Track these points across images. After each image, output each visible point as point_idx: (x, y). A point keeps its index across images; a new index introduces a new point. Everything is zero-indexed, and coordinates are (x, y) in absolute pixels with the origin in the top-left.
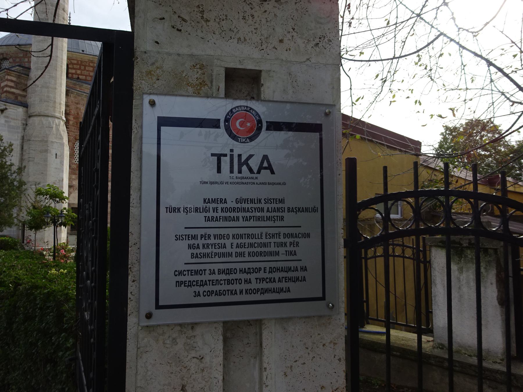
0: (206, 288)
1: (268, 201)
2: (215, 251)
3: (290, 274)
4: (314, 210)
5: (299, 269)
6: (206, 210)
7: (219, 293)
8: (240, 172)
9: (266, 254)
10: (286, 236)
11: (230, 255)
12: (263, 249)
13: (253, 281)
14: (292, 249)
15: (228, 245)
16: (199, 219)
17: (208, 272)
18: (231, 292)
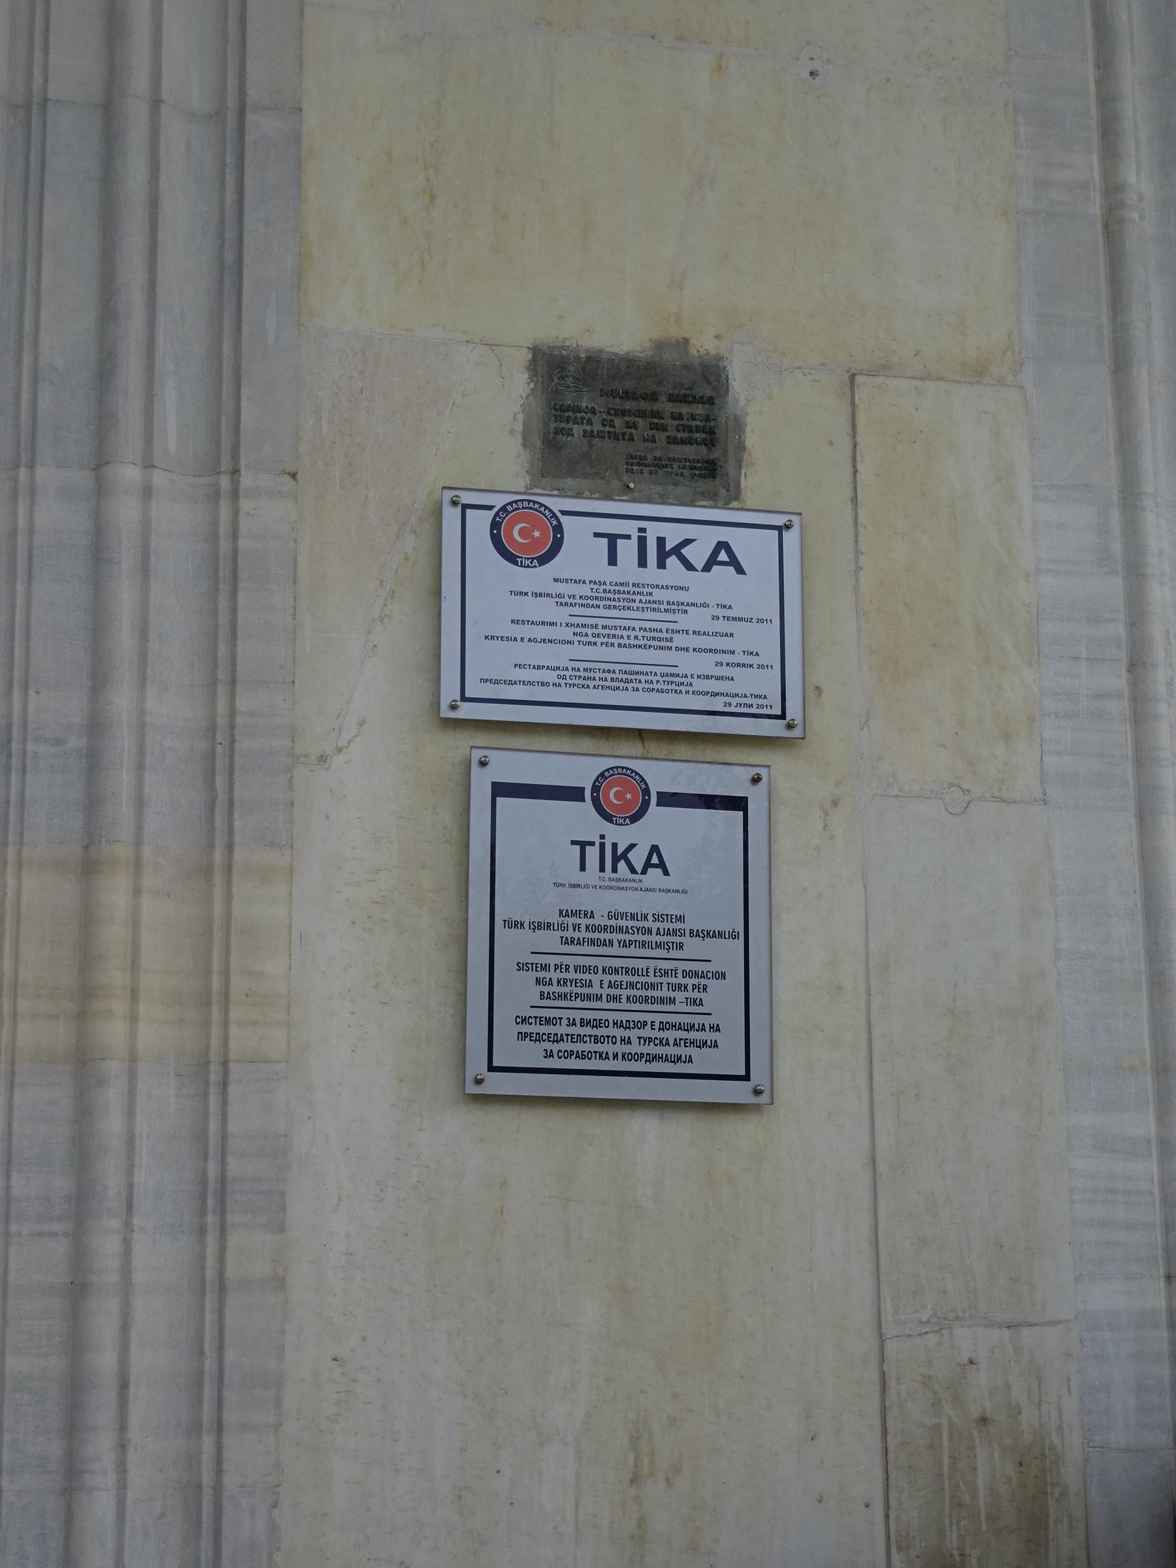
0: (563, 1046)
1: (658, 917)
2: (576, 990)
3: (692, 1035)
4: (733, 935)
5: (707, 1028)
6: (563, 927)
7: (581, 1056)
8: (615, 870)
9: (654, 1000)
10: (686, 974)
11: (599, 998)
12: (650, 993)
13: (635, 1041)
14: (695, 995)
15: (596, 983)
16: (550, 940)
17: (565, 1022)
18: (601, 1056)
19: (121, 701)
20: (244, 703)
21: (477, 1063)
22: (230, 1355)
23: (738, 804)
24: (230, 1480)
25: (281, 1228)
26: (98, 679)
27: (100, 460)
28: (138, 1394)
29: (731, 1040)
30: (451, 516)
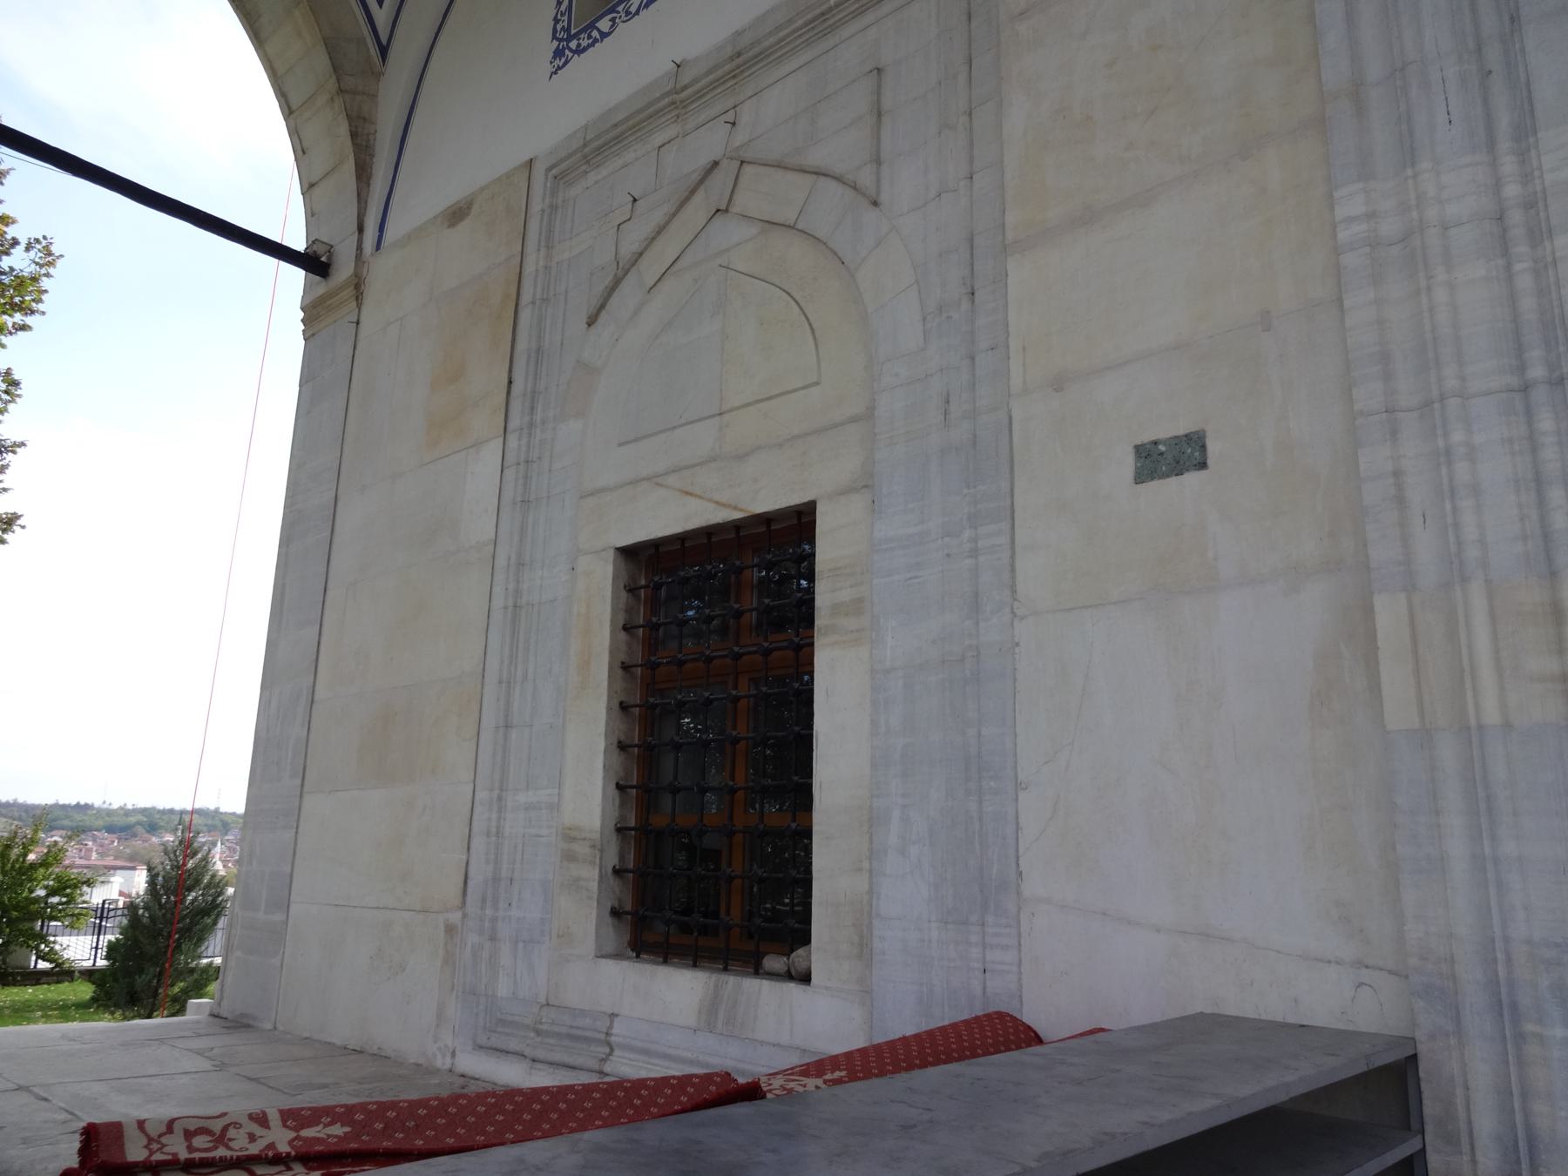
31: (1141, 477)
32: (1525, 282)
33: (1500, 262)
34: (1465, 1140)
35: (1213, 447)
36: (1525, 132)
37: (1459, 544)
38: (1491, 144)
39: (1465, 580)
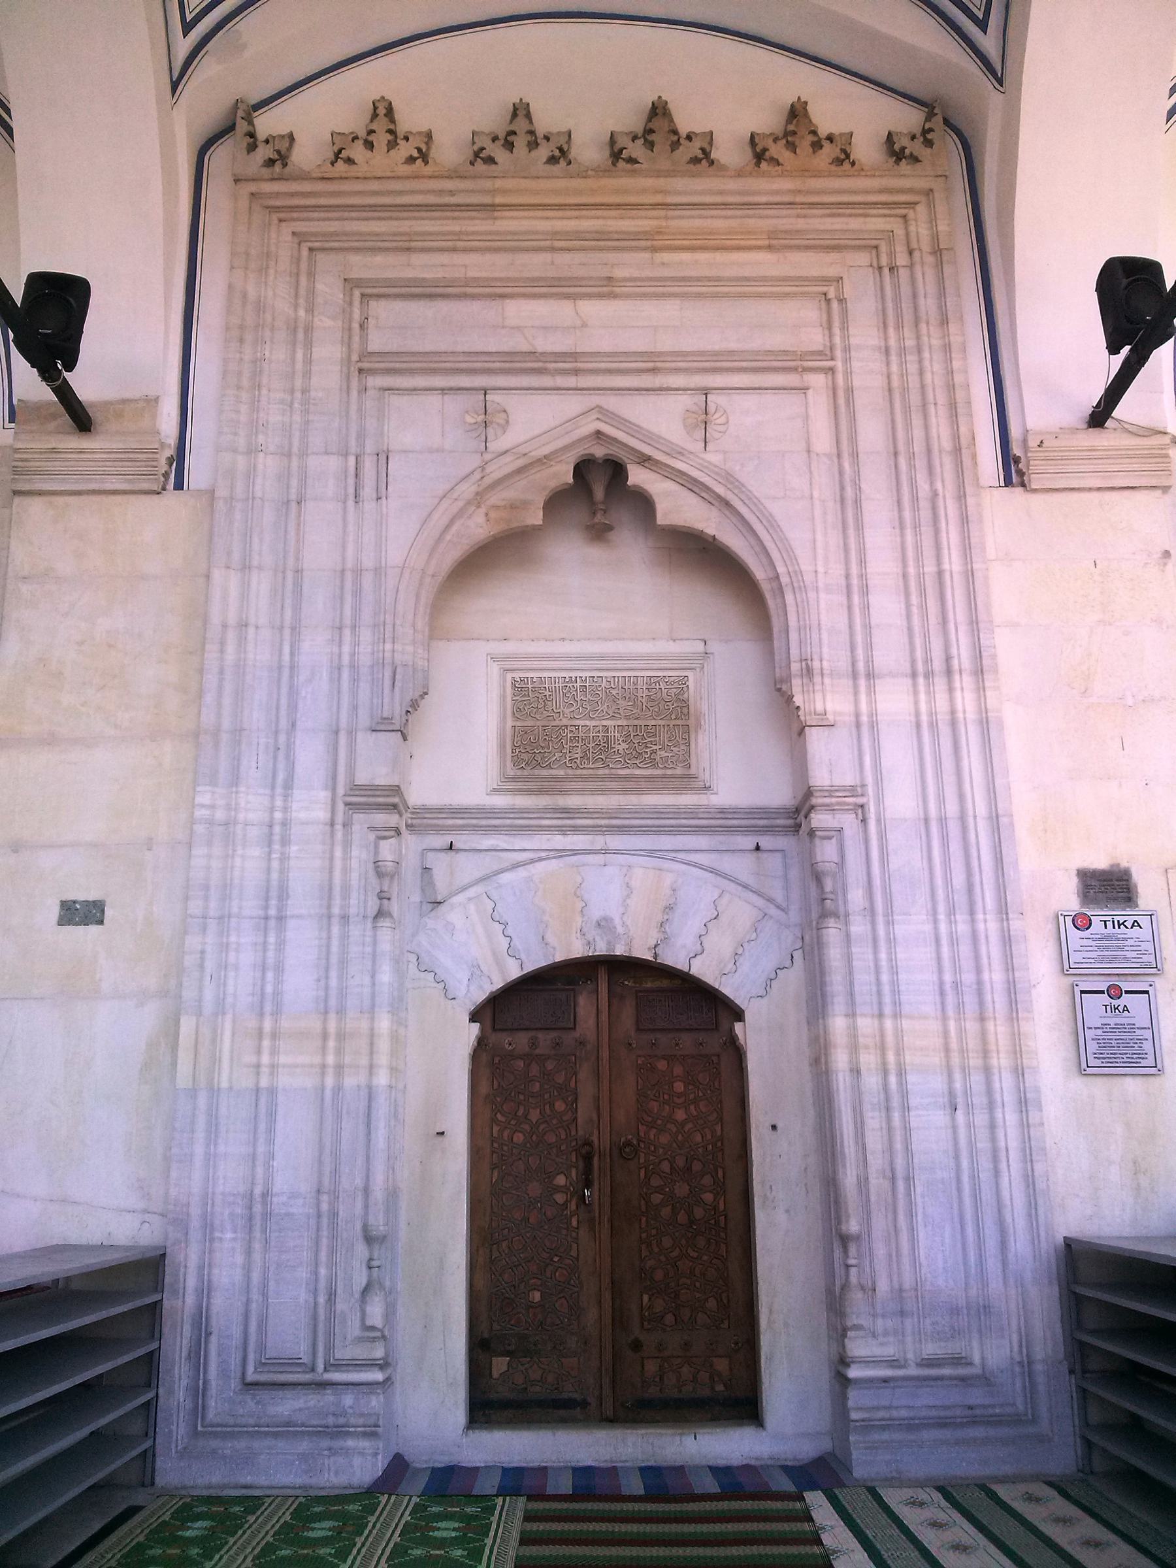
16: (1099, 1032)
19: (986, 976)
20: (1017, 974)
21: (1084, 1066)
22: (1033, 1143)
23: (1147, 992)
24: (1036, 1174)
25: (1041, 1111)
26: (978, 970)
27: (972, 912)
28: (1011, 1152)
29: (1151, 1057)
30: (1061, 918)
31: (61, 922)
32: (275, 864)
33: (267, 849)
34: (181, 1291)
35: (109, 913)
36: (288, 785)
37: (224, 994)
38: (273, 788)
39: (224, 1013)
